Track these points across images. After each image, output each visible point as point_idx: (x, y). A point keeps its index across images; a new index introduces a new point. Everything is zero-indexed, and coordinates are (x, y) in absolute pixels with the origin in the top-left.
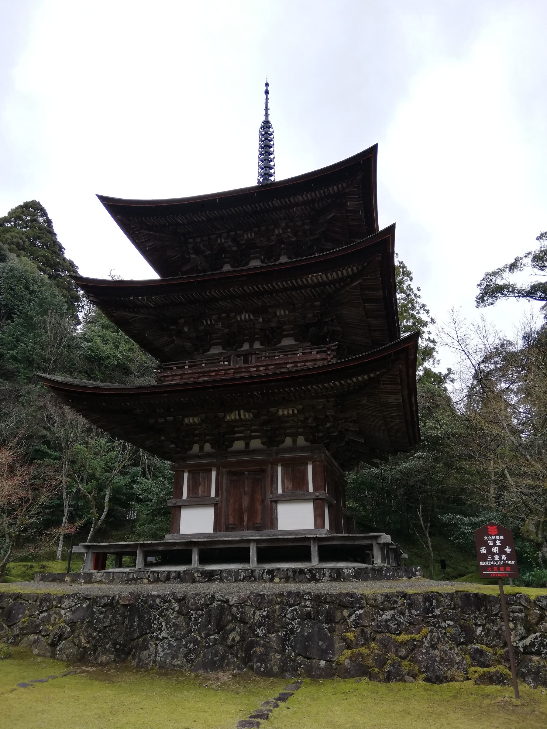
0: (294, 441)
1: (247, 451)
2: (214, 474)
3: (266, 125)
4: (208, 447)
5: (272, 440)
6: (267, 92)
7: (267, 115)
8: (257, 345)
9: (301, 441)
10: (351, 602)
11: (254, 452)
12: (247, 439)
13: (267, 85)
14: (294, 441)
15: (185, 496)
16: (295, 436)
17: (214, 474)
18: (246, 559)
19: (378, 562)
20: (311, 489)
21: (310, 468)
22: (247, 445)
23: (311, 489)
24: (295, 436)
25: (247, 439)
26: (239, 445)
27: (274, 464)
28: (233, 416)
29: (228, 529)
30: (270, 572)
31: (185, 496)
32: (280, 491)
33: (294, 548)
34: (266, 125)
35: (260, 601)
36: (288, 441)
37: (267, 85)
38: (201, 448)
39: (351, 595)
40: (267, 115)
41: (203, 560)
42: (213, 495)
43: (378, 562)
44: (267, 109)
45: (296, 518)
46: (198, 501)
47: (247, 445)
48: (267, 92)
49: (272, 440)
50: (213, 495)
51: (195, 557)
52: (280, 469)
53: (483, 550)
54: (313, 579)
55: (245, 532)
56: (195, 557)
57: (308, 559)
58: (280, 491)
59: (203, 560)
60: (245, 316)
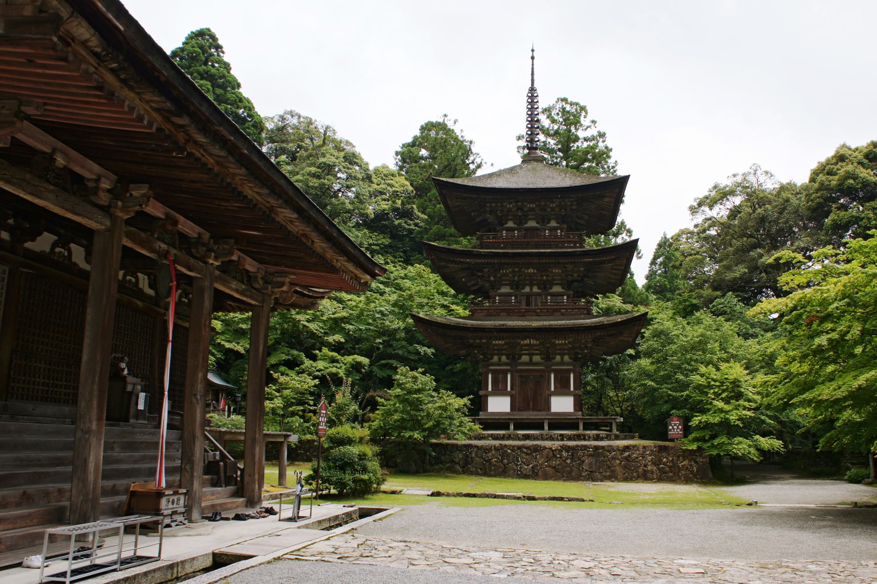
0: (562, 359)
1: (531, 363)
2: (509, 376)
3: (532, 90)
4: (504, 358)
5: (548, 358)
6: (533, 58)
7: (533, 80)
8: (535, 289)
9: (566, 358)
10: (610, 449)
11: (537, 364)
12: (531, 355)
13: (533, 51)
14: (562, 359)
15: (490, 389)
16: (562, 355)
17: (509, 376)
18: (542, 428)
19: (615, 431)
20: (572, 389)
21: (572, 376)
22: (531, 359)
23: (572, 389)
24: (562, 355)
25: (531, 355)
26: (525, 358)
27: (550, 373)
28: (527, 341)
29: (520, 410)
30: (561, 435)
31: (490, 389)
32: (553, 389)
33: (561, 422)
34: (532, 90)
35: (567, 449)
36: (558, 358)
37: (533, 51)
38: (500, 359)
39: (611, 446)
40: (533, 80)
41: (515, 428)
42: (509, 389)
43: (615, 431)
44: (533, 74)
45: (563, 405)
46: (499, 391)
47: (531, 359)
48: (533, 58)
49: (548, 358)
50: (509, 389)
51: (512, 427)
52: (552, 376)
53: (670, 427)
54: (585, 439)
55: (531, 412)
56: (512, 427)
57: (578, 429)
58: (553, 389)
59: (515, 428)
60: (531, 271)
